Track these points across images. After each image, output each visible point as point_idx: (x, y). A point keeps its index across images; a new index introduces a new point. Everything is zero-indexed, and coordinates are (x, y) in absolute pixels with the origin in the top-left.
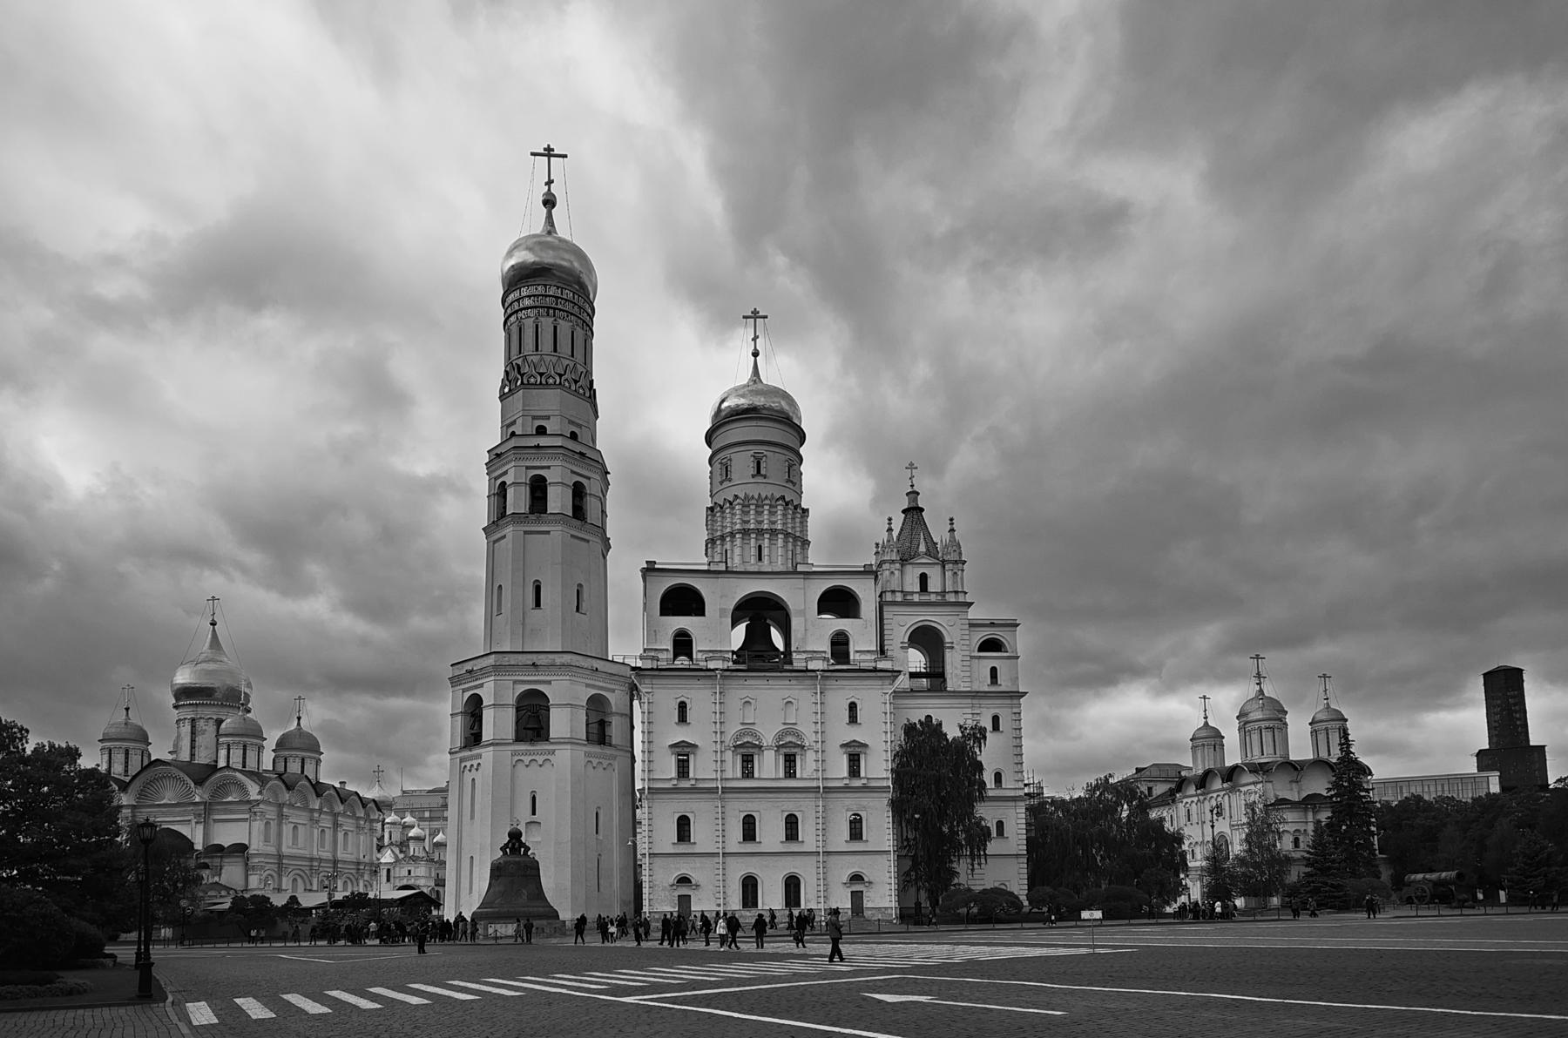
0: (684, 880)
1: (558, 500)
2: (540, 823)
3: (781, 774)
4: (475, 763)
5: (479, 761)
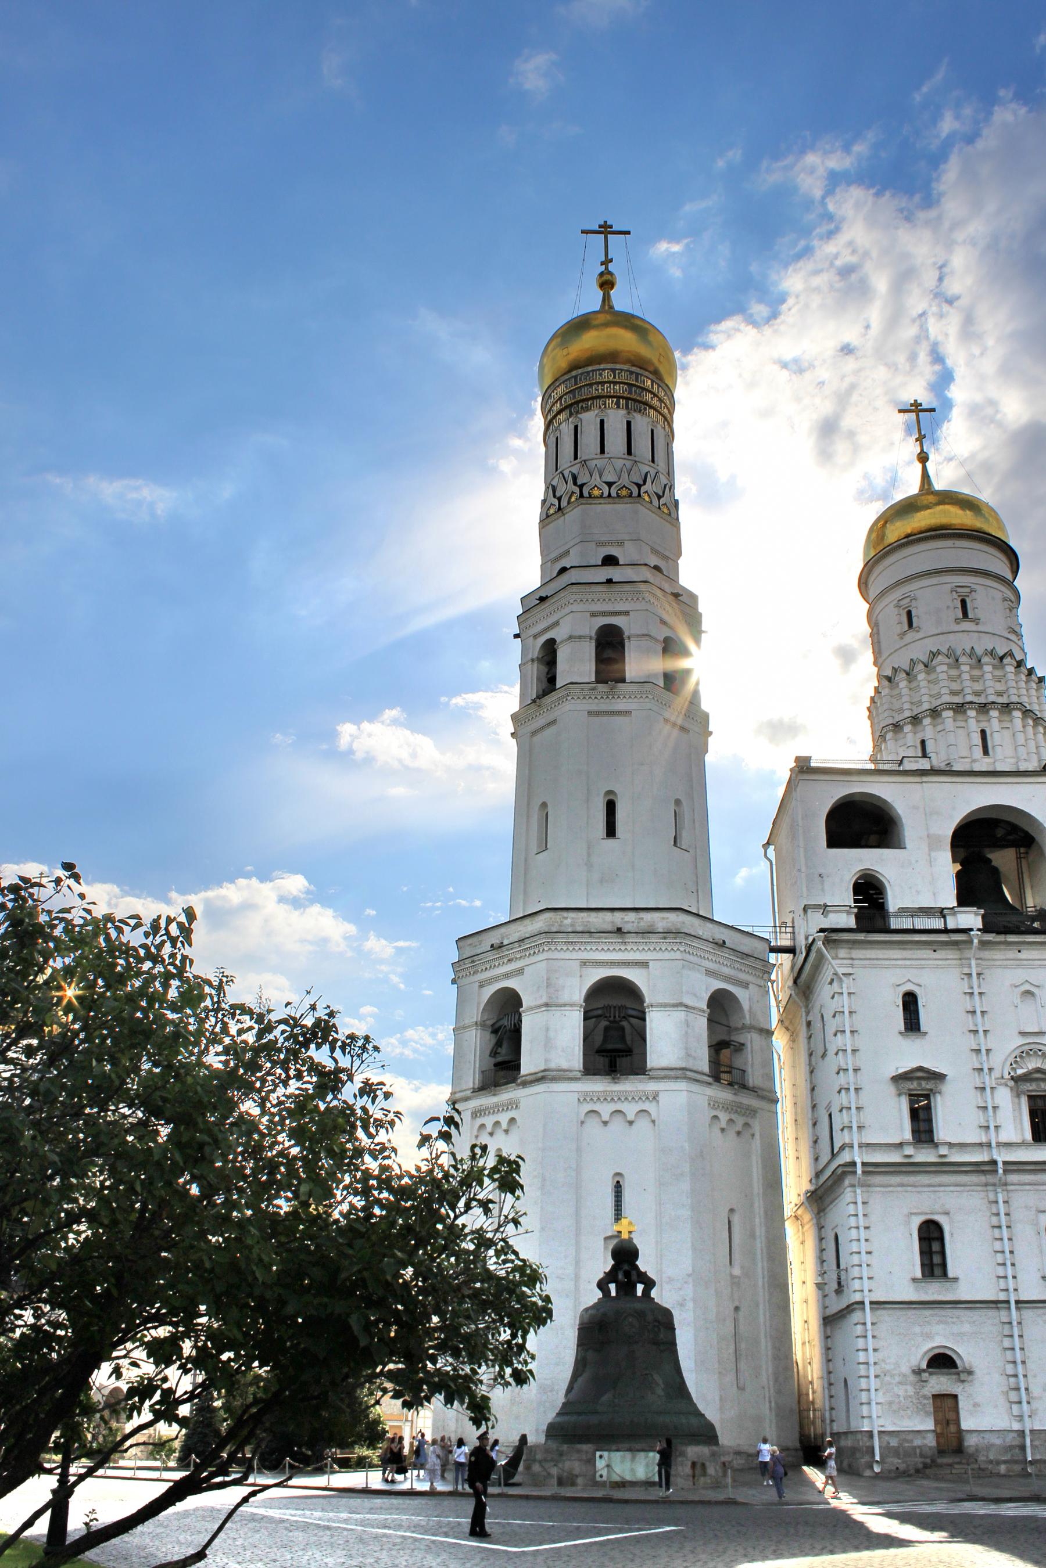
4: (504, 1118)
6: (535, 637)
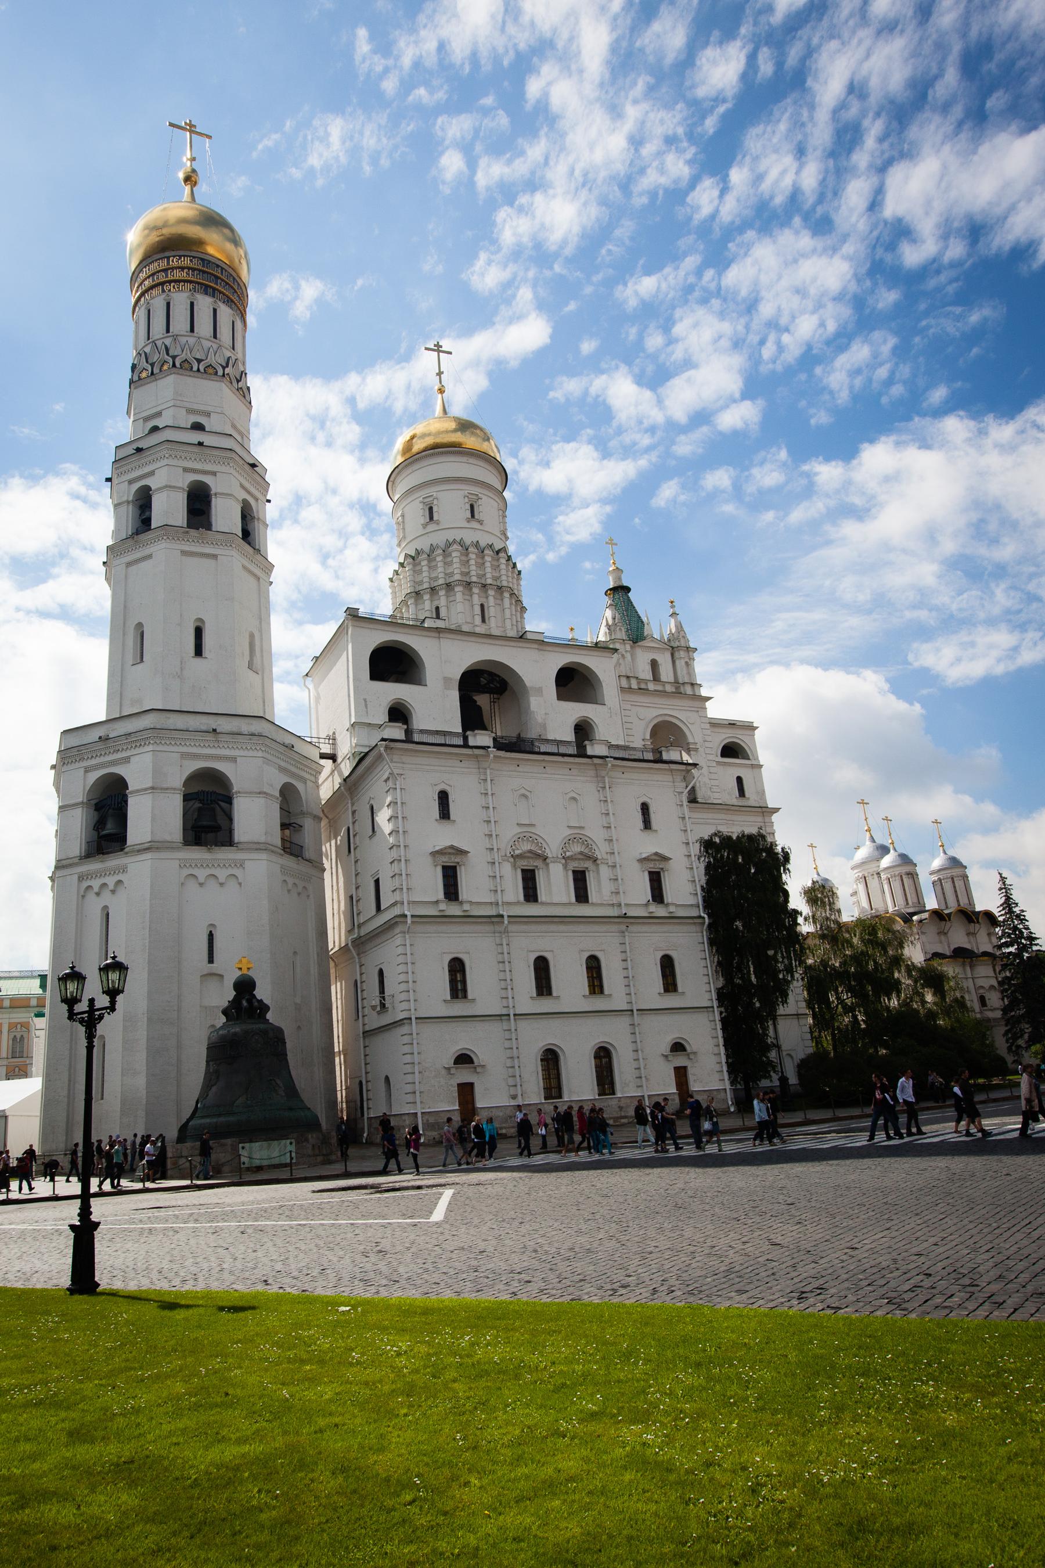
2: (221, 976)
4: (111, 881)
5: (120, 877)
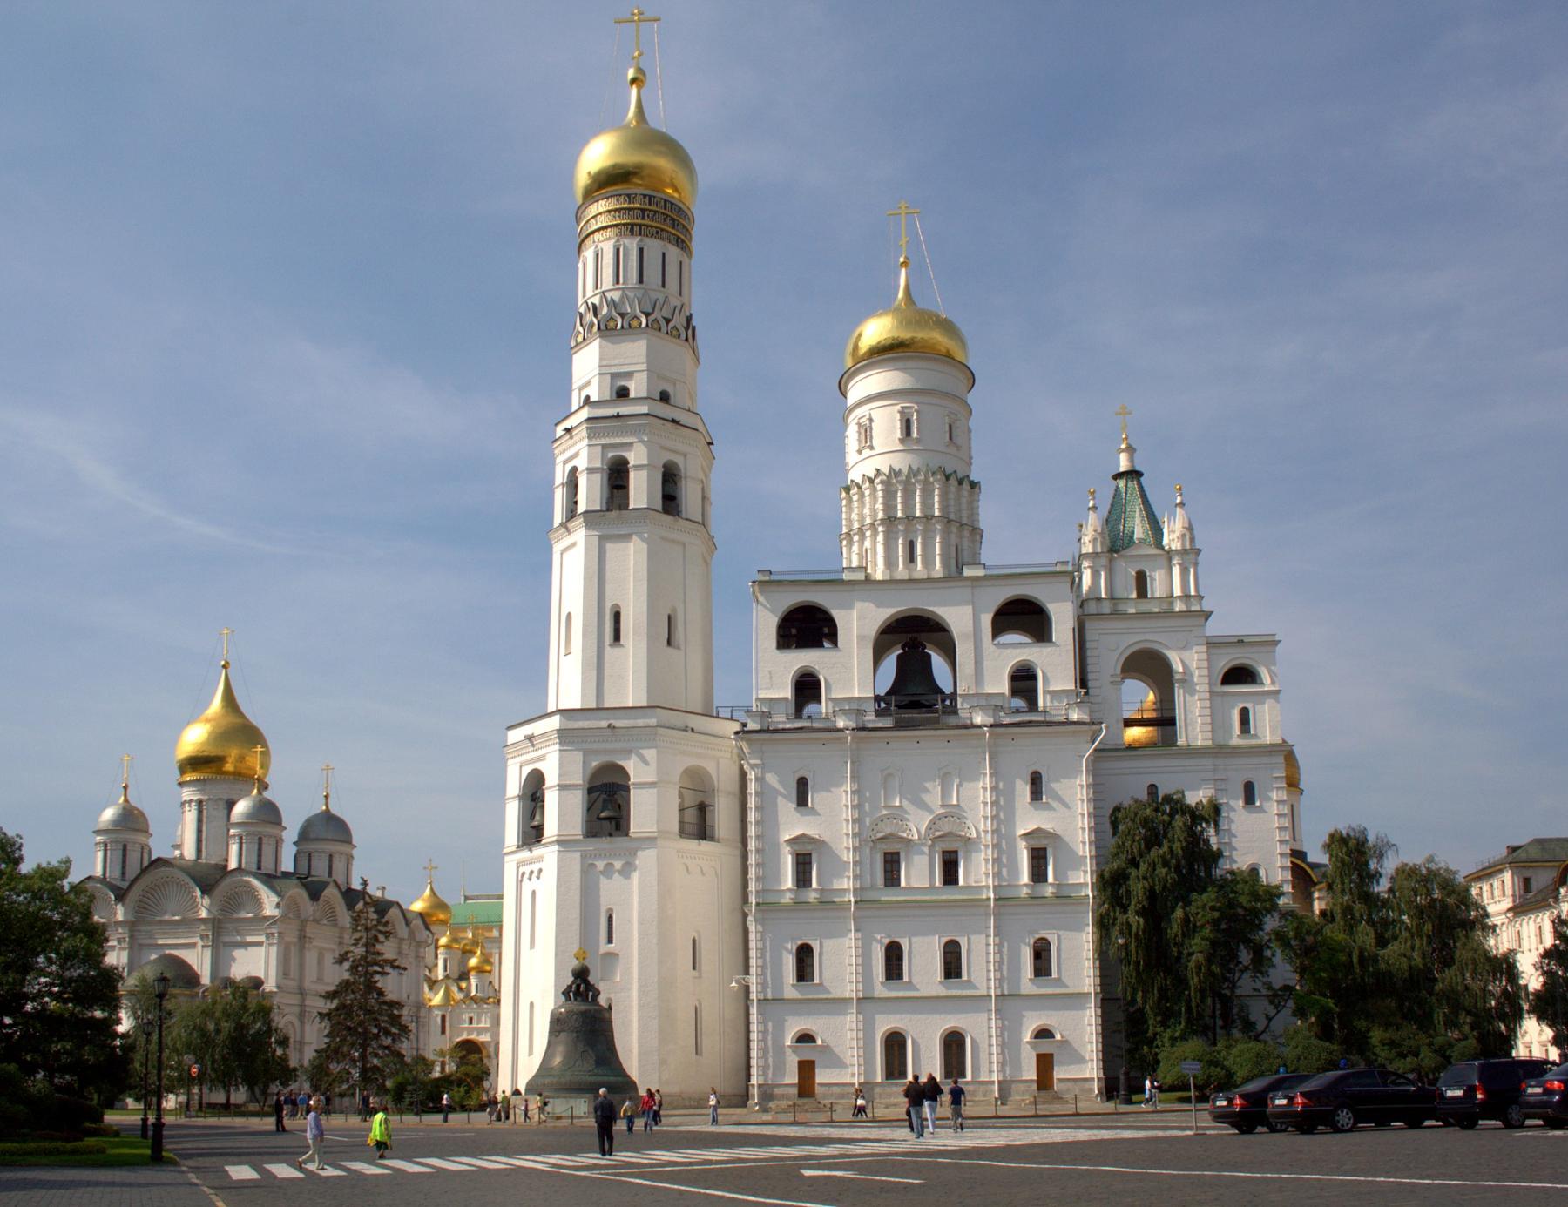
0: (805, 1038)
1: (641, 490)
3: (938, 882)
4: (535, 867)
6: (565, 463)
